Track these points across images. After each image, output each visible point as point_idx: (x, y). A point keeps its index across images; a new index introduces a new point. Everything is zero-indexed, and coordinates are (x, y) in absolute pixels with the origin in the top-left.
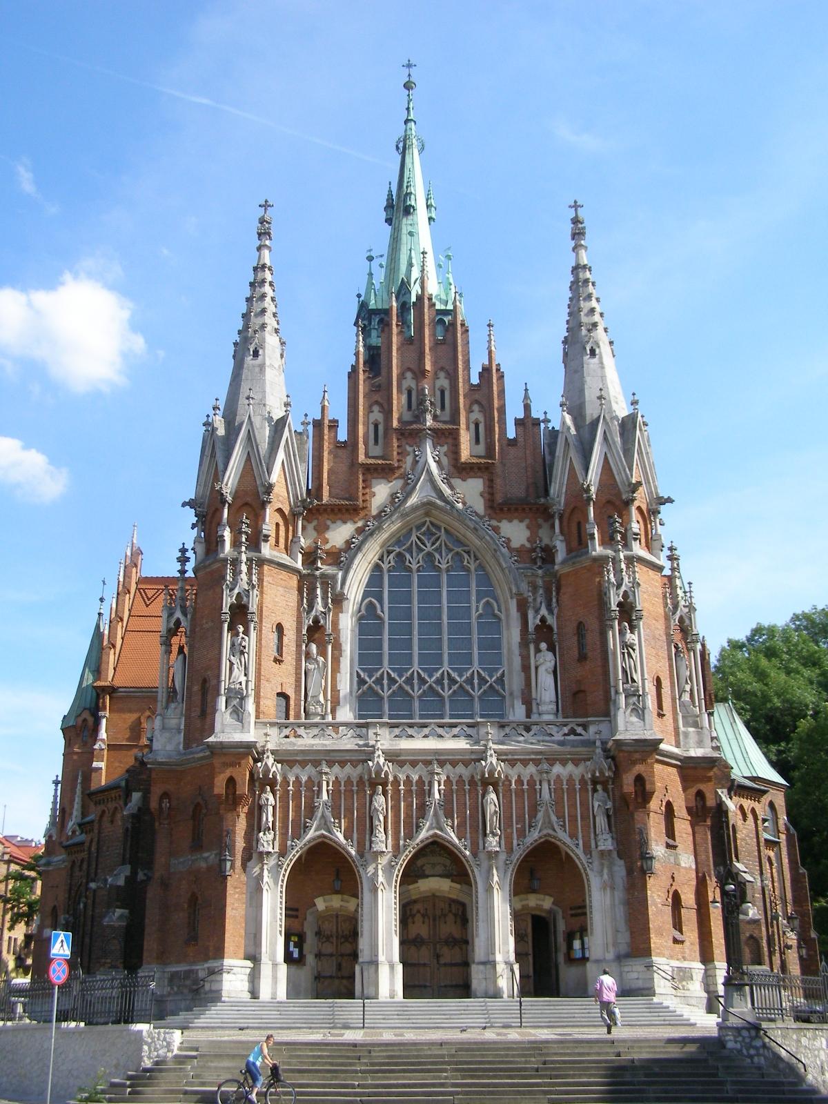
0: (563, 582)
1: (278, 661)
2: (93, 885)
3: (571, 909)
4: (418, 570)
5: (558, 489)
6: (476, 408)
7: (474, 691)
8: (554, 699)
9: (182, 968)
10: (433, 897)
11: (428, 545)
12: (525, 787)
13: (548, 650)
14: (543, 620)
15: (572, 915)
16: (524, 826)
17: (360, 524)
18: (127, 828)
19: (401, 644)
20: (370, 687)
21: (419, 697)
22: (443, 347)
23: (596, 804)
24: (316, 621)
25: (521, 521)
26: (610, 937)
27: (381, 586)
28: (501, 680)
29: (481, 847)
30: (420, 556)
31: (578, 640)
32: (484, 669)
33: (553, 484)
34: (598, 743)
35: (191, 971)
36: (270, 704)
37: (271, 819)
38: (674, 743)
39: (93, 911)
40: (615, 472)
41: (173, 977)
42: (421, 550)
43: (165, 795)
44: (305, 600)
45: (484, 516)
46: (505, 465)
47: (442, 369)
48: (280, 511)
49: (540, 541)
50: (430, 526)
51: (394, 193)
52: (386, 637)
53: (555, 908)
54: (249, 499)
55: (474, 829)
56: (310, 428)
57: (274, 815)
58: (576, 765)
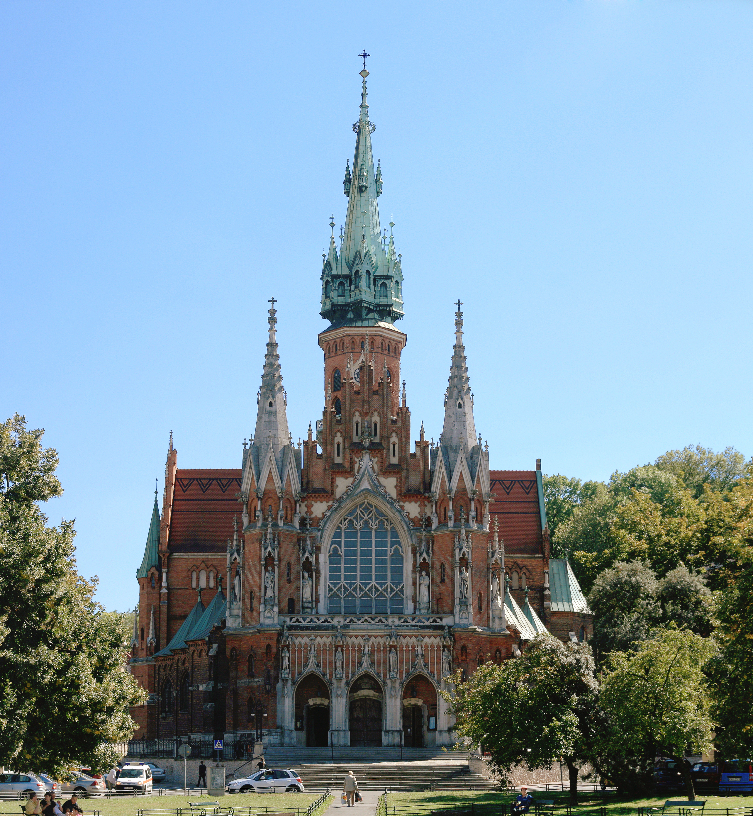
0: (435, 540)
1: (289, 581)
2: (190, 688)
3: (432, 705)
4: (360, 529)
5: (436, 487)
6: (394, 434)
7: (388, 595)
8: (427, 601)
9: (246, 732)
10: (365, 699)
11: (366, 515)
12: (410, 648)
13: (426, 575)
14: (424, 559)
15: (432, 709)
16: (409, 668)
17: (330, 503)
18: (211, 662)
19: (350, 570)
20: (335, 592)
21: (360, 597)
22: (377, 396)
23: (444, 657)
24: (307, 558)
25: (416, 503)
26: (446, 720)
27: (340, 537)
28: (401, 590)
29: (388, 677)
30: (362, 522)
31: (441, 572)
32: (393, 584)
33: (433, 485)
34: (446, 627)
35: (251, 734)
36: (285, 605)
37: (288, 663)
38: (486, 625)
39: (192, 702)
40: (465, 482)
41: (242, 736)
42: (362, 518)
43: (234, 649)
44: (301, 548)
45: (396, 500)
46: (408, 470)
47: (375, 410)
48: (288, 499)
49: (425, 514)
50: (368, 505)
51: (351, 173)
52: (343, 566)
53: (423, 705)
54: (271, 495)
55: (385, 668)
56: (302, 447)
57: (289, 661)
58: (436, 638)
